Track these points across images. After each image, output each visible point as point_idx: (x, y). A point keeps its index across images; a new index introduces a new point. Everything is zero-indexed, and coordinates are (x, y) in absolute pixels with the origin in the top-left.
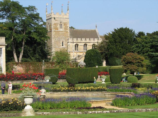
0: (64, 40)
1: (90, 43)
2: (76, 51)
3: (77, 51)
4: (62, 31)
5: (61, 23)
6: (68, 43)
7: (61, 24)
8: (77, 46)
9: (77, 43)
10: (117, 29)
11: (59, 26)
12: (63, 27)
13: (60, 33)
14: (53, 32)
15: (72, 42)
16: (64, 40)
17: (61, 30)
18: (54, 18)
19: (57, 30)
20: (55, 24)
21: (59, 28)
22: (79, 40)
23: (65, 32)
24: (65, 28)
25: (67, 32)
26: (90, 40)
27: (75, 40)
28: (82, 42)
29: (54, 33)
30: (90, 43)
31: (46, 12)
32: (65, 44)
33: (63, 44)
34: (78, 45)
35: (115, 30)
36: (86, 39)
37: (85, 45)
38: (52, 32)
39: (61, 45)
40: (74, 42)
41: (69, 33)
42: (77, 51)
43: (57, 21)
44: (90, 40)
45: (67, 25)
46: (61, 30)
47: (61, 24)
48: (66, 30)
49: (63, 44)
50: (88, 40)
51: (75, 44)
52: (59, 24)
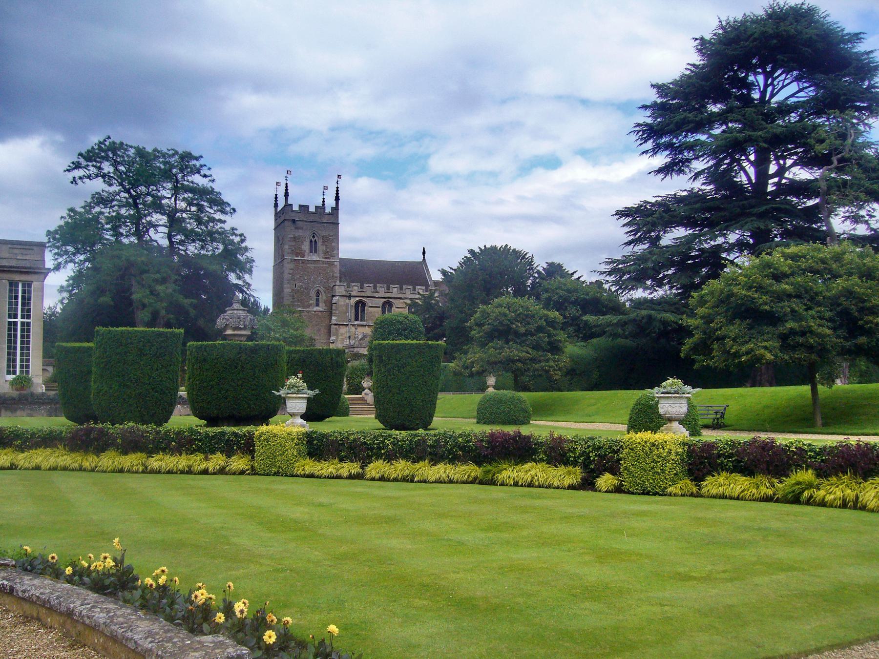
0: (322, 289)
1: (401, 298)
2: (356, 323)
3: (362, 323)
4: (315, 262)
5: (314, 237)
6: (333, 296)
7: (313, 240)
8: (360, 306)
9: (363, 299)
10: (477, 250)
11: (306, 247)
12: (321, 247)
13: (312, 266)
14: (288, 263)
15: (344, 293)
16: (322, 289)
17: (315, 257)
18: (294, 221)
19: (299, 258)
20: (295, 239)
21: (308, 251)
22: (368, 289)
23: (327, 265)
24: (326, 253)
25: (331, 264)
26: (401, 289)
27: (355, 290)
28: (376, 295)
29: (292, 266)
30: (401, 298)
31: (276, 205)
32: (325, 302)
33: (317, 300)
34: (364, 304)
35: (471, 252)
36: (388, 288)
37: (387, 305)
38: (285, 263)
39: (311, 302)
40: (353, 294)
41: (338, 267)
42: (362, 323)
43: (300, 231)
44: (401, 289)
45: (333, 244)
46: (315, 257)
47: (313, 240)
48: (329, 258)
49: (317, 300)
50: (395, 291)
51: (353, 301)
52: (308, 240)
